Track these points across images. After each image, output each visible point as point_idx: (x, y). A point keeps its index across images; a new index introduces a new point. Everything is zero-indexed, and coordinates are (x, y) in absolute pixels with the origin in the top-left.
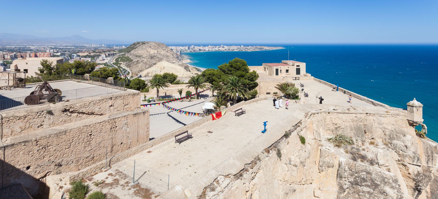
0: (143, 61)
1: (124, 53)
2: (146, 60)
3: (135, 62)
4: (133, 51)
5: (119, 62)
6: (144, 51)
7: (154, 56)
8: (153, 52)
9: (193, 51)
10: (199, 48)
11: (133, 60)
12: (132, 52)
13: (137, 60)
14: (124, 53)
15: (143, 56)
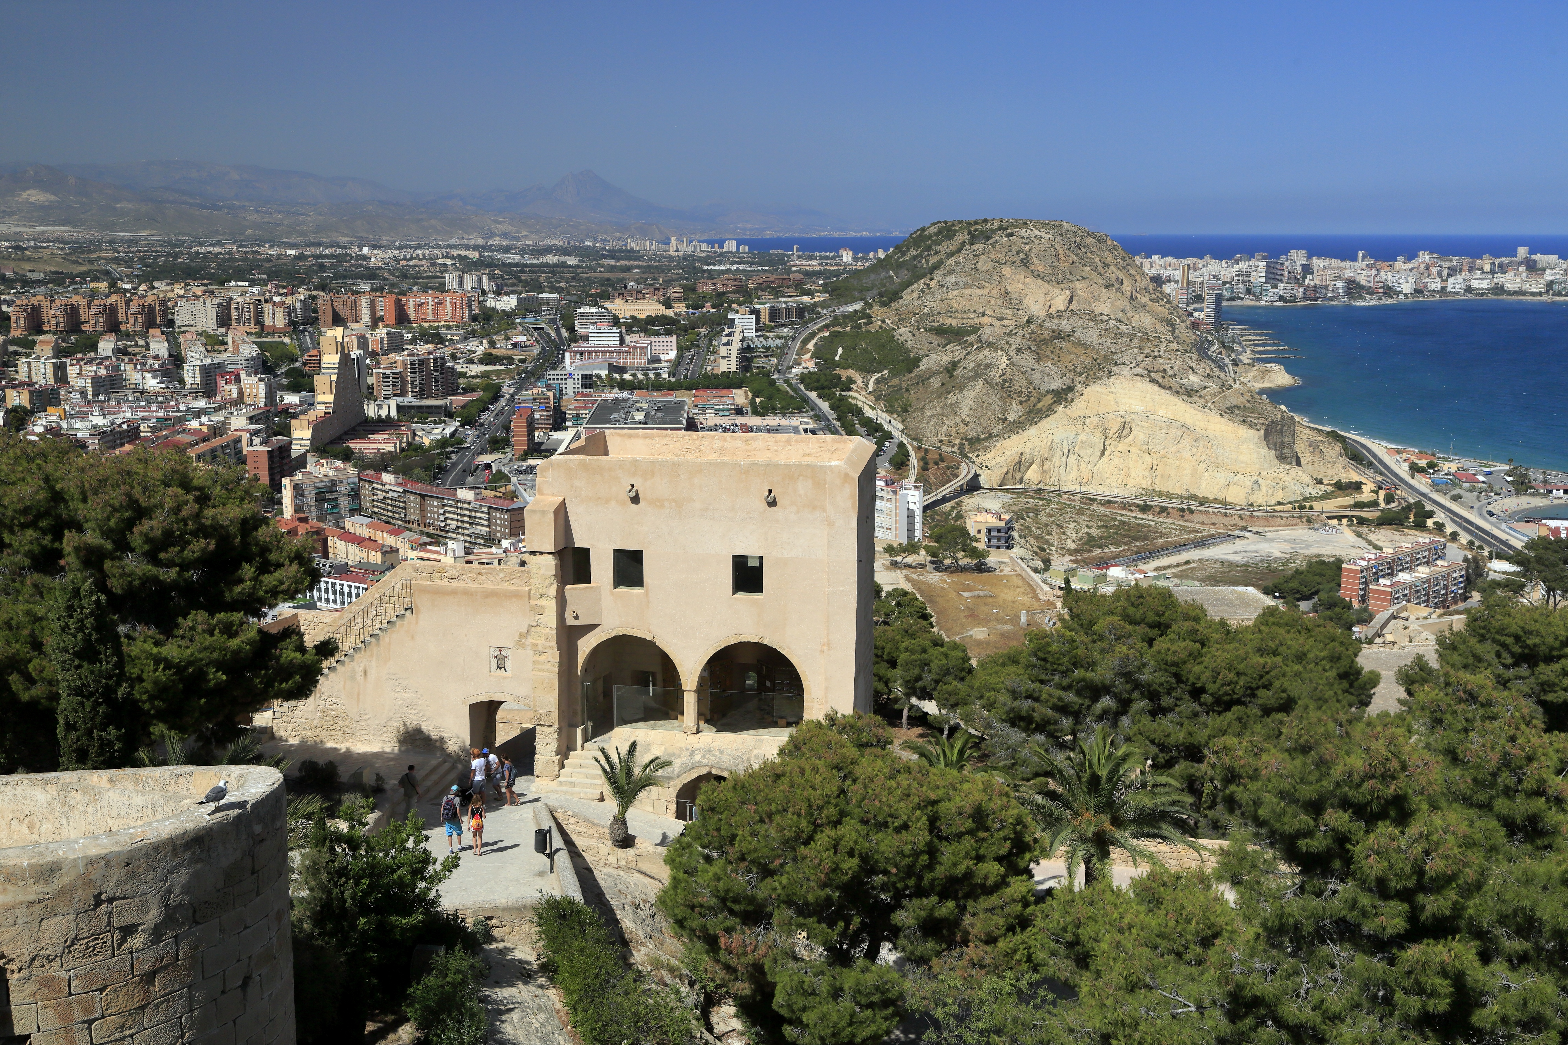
0: (988, 366)
1: (857, 306)
2: (1004, 361)
3: (933, 374)
6: (985, 292)
7: (1059, 335)
8: (1041, 300)
9: (1300, 293)
10: (1349, 274)
11: (917, 360)
12: (910, 296)
13: (945, 360)
14: (857, 306)
15: (987, 334)
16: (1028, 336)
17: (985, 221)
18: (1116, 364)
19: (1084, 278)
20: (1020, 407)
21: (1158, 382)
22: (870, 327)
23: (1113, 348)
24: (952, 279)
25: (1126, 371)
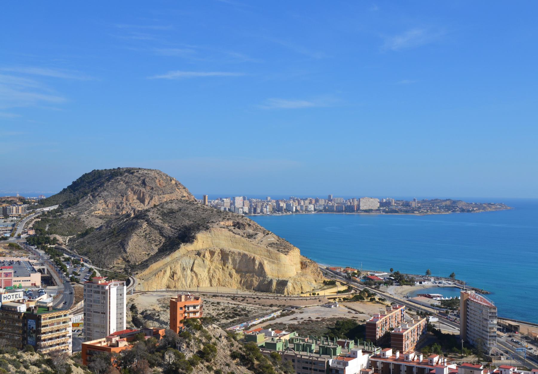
1: (56, 207)
4: (86, 201)
5: (47, 236)
14: (56, 207)
16: (156, 212)
17: (119, 168)
18: (208, 223)
19: (171, 193)
20: (156, 247)
21: (232, 231)
22: (63, 216)
23: (203, 216)
24: (106, 193)
25: (215, 225)
